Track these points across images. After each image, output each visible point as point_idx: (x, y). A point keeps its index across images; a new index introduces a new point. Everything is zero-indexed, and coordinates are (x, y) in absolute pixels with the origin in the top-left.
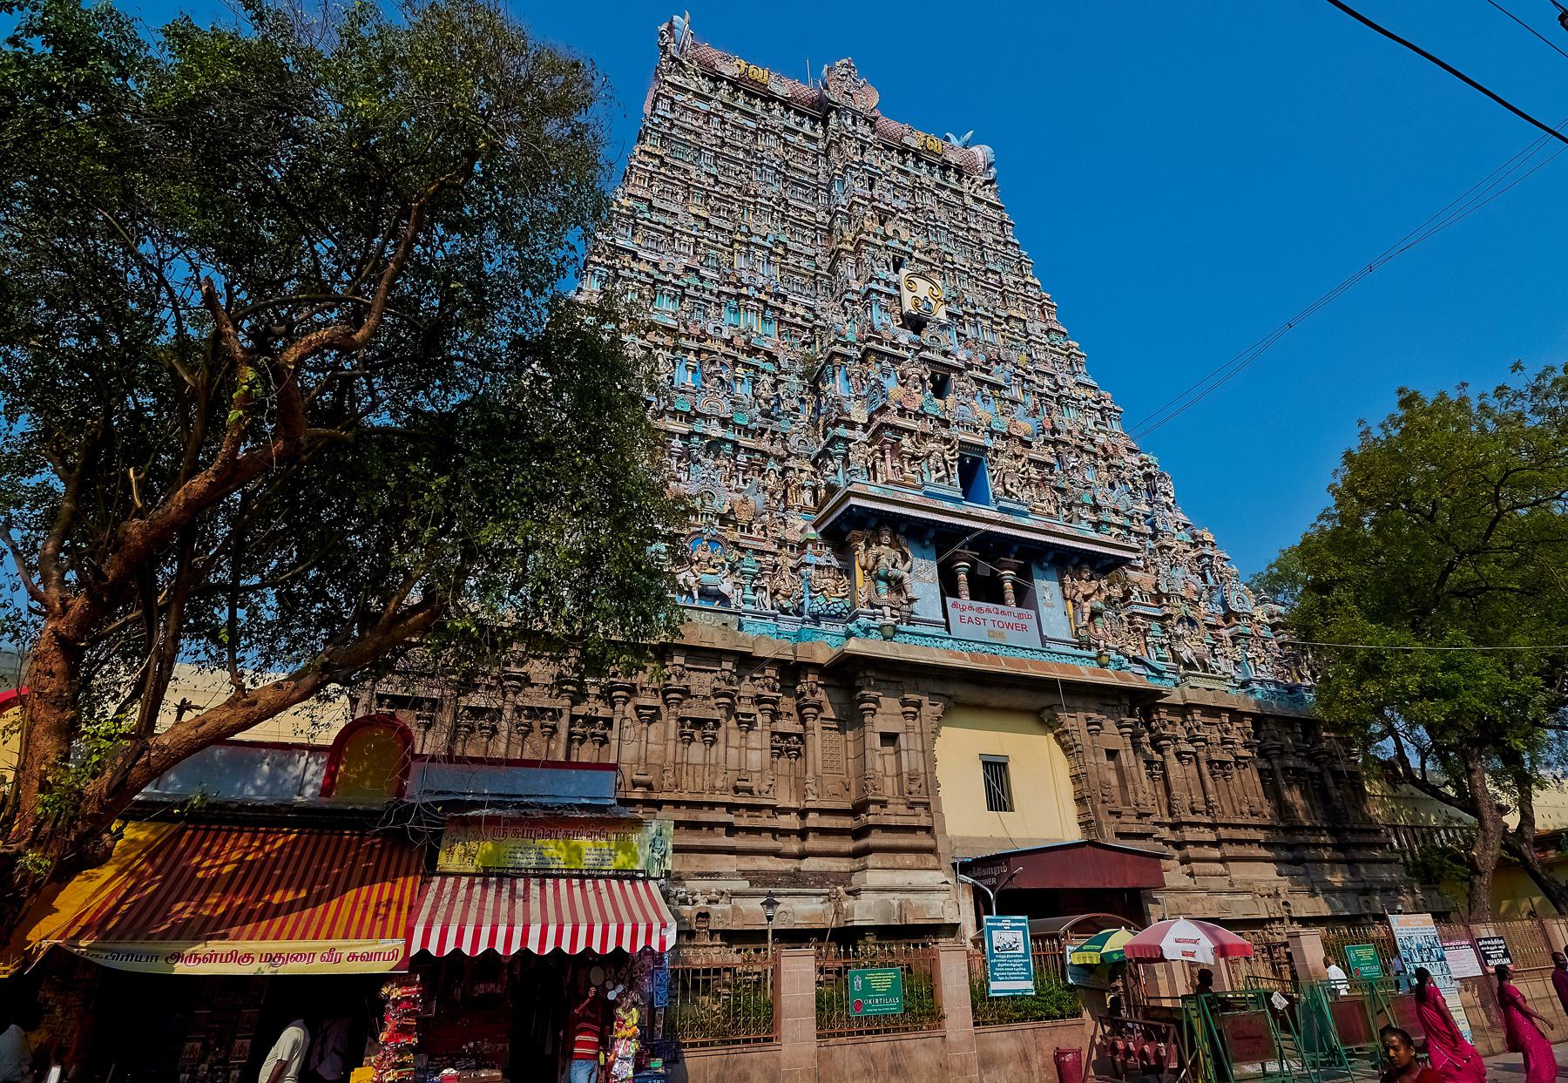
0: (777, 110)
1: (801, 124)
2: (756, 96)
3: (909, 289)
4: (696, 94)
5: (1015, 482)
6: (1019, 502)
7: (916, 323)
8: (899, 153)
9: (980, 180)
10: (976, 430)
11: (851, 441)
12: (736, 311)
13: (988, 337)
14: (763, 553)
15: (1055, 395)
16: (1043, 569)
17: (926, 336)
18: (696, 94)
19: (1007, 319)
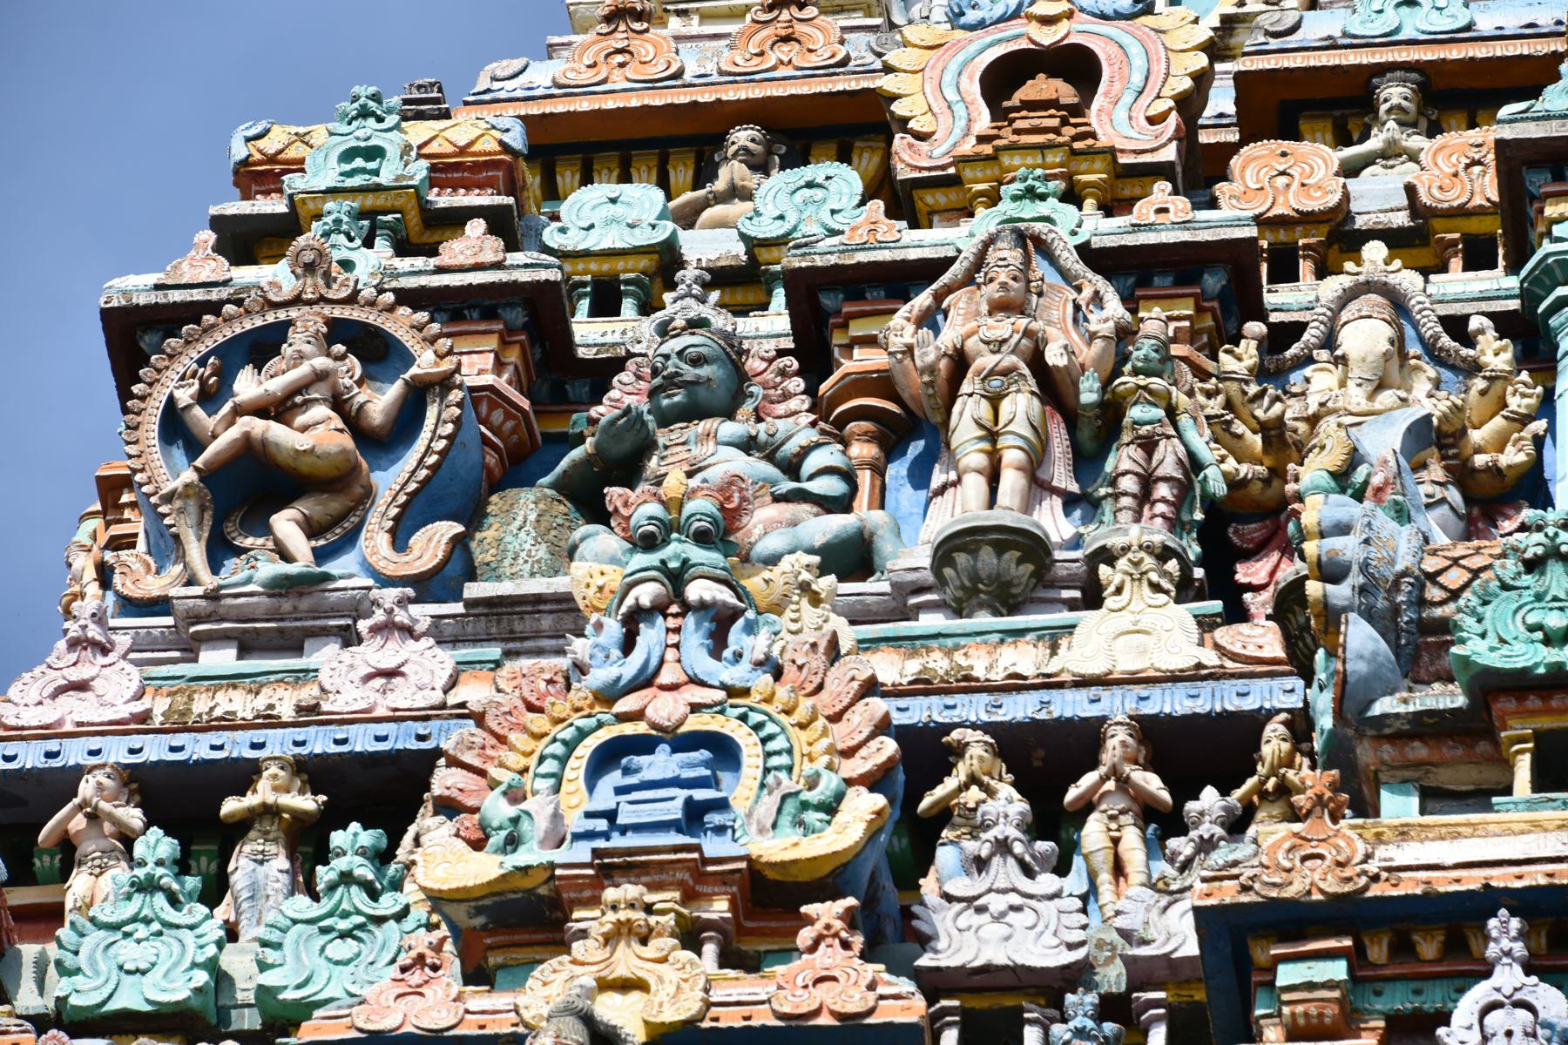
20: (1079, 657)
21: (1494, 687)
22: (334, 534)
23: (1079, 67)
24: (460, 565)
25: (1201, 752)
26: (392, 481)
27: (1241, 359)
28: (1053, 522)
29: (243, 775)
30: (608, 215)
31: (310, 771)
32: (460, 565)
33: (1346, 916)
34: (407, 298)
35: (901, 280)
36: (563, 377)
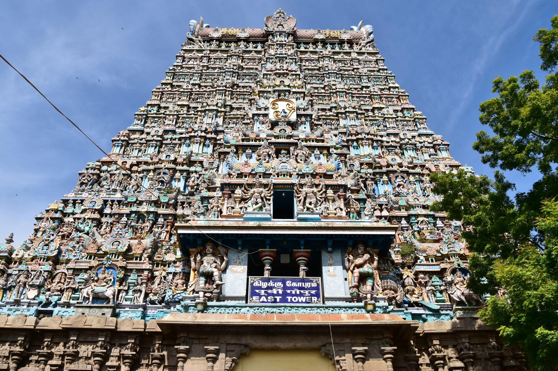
0: (242, 45)
1: (256, 47)
2: (231, 42)
3: (274, 108)
4: (198, 51)
5: (313, 200)
6: (313, 213)
7: (274, 124)
8: (313, 44)
9: (363, 43)
10: (291, 176)
11: (211, 198)
12: (189, 146)
13: (353, 122)
14: (143, 270)
15: (399, 145)
16: (330, 252)
17: (277, 130)
18: (198, 51)
19: (373, 110)
20: (116, 196)
21: (129, 202)
22: (86, 186)
23: (126, 162)
24: (92, 188)
25: (119, 202)
26: (90, 183)
27: (129, 179)
28: (118, 188)
29: (77, 200)
30: (104, 168)
31: (80, 200)
32: (92, 188)
33: (118, 214)
34: (91, 174)
35: (115, 174)
36: (99, 176)
